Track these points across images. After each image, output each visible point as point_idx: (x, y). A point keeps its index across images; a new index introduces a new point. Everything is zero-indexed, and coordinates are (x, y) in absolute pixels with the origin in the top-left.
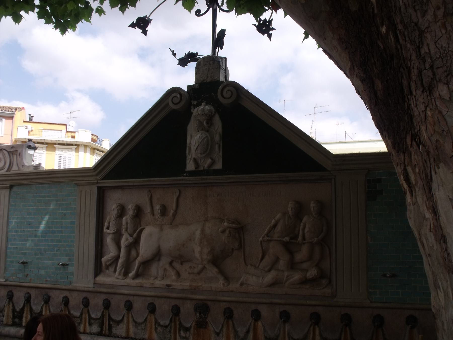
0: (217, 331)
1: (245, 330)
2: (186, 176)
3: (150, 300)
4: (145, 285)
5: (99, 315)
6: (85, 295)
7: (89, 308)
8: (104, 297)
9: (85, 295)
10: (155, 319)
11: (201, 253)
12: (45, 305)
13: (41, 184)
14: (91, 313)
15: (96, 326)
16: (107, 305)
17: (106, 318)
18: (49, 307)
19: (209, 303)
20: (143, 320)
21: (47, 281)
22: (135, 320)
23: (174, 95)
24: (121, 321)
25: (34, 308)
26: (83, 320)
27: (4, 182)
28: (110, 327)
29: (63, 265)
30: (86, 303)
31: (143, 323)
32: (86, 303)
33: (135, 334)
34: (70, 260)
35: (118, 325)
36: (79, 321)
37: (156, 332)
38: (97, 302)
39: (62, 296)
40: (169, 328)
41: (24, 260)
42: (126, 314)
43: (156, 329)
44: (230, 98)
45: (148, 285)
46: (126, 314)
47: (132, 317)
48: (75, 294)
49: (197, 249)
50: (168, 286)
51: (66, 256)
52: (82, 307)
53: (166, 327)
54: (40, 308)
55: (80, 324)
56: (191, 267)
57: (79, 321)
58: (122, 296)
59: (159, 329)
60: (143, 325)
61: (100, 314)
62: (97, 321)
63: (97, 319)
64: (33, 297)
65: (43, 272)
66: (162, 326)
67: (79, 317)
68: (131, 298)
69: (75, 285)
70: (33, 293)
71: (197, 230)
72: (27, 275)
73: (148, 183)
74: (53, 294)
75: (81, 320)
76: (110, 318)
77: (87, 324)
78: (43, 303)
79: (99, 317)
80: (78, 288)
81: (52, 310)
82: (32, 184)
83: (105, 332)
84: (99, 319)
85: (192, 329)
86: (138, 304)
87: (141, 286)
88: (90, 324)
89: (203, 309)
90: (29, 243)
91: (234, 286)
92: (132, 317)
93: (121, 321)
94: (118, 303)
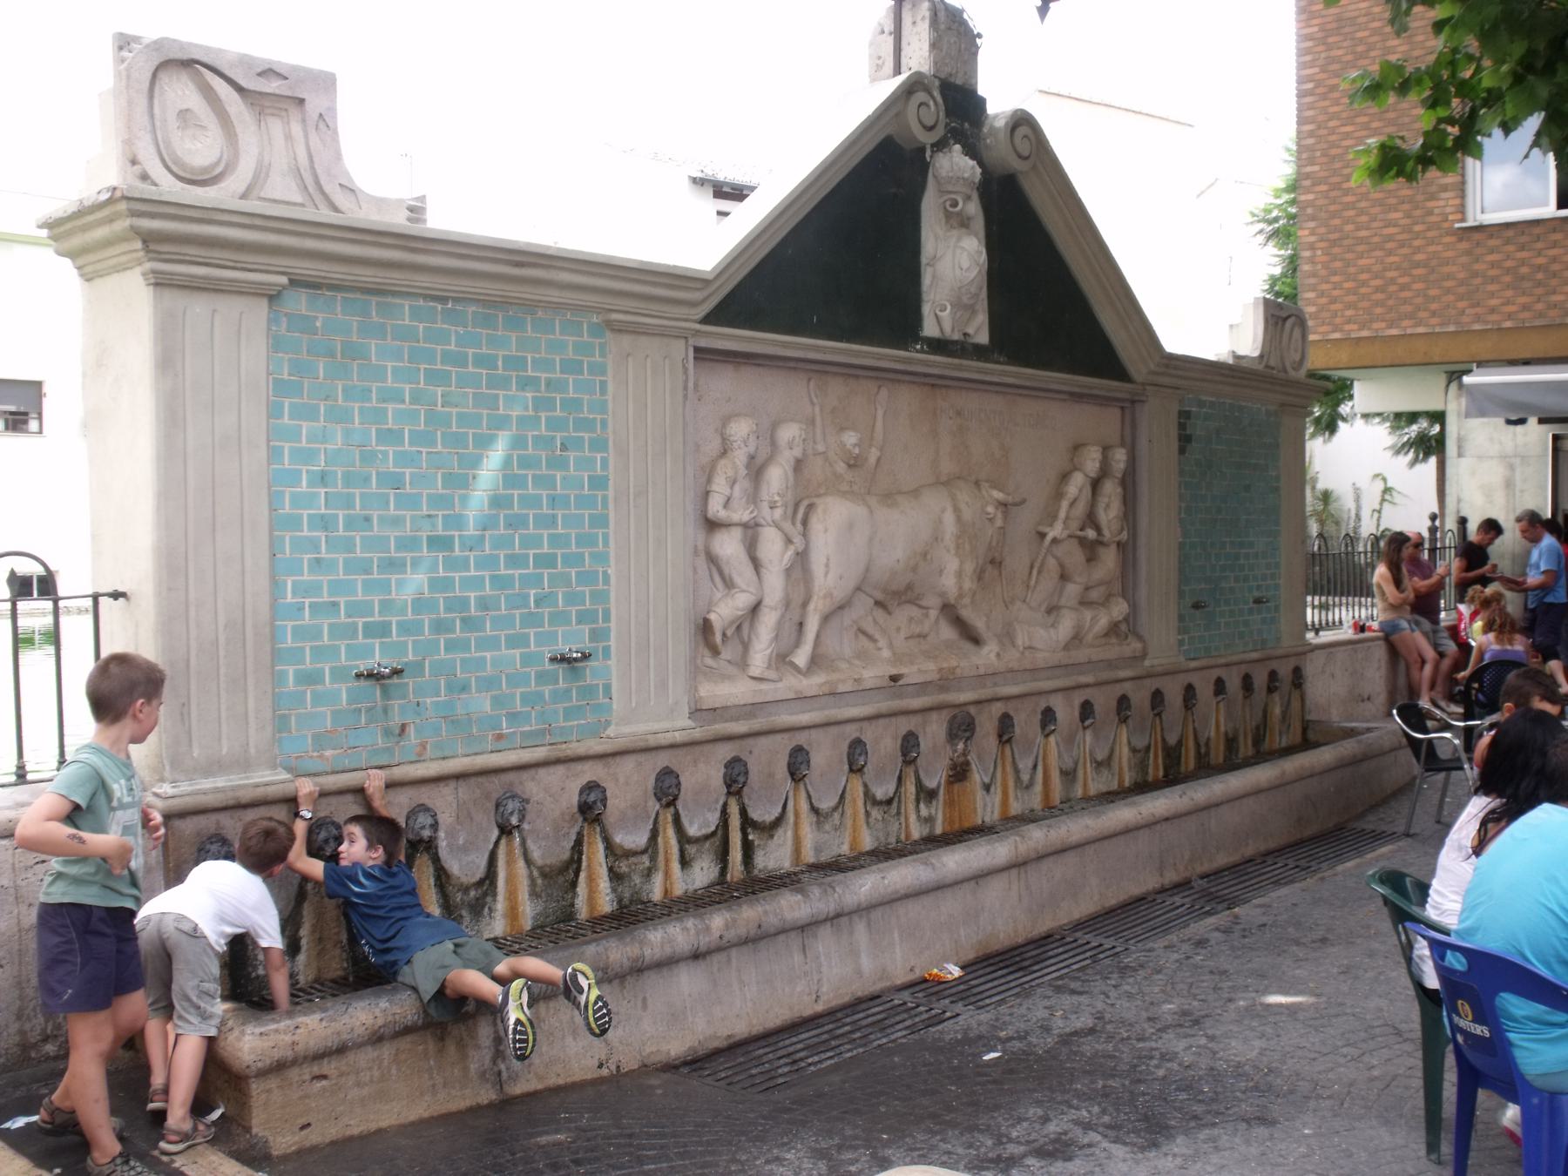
0: (987, 780)
1: (1030, 764)
2: (922, 351)
3: (852, 731)
4: (841, 688)
5: (713, 819)
6: (662, 760)
7: (680, 805)
8: (725, 752)
9: (662, 760)
10: (865, 786)
11: (959, 574)
12: (503, 841)
13: (443, 300)
14: (685, 821)
15: (705, 864)
16: (735, 780)
17: (735, 822)
18: (523, 843)
19: (972, 710)
20: (837, 799)
21: (500, 737)
22: (816, 804)
23: (921, 96)
24: (778, 822)
25: (454, 866)
26: (661, 858)
27: (192, 251)
28: (748, 848)
29: (563, 659)
30: (667, 790)
31: (835, 809)
32: (667, 790)
33: (818, 850)
34: (596, 635)
35: (772, 837)
36: (647, 864)
37: (868, 823)
38: (703, 775)
39: (575, 787)
40: (895, 804)
41: (377, 659)
42: (791, 794)
43: (868, 814)
44: (1020, 156)
45: (848, 687)
46: (791, 794)
47: (809, 797)
48: (628, 765)
49: (952, 564)
50: (894, 679)
51: (579, 622)
52: (654, 806)
53: (889, 802)
54: (483, 862)
55: (648, 873)
56: (911, 619)
57: (647, 864)
58: (778, 737)
59: (876, 813)
60: (836, 815)
61: (717, 814)
62: (707, 844)
63: (707, 837)
64: (445, 819)
65: (481, 703)
66: (880, 803)
67: (644, 852)
68: (801, 739)
69: (626, 730)
70: (444, 802)
71: (943, 511)
72: (403, 728)
73: (812, 355)
74: (533, 786)
75: (653, 859)
76: (747, 822)
77: (675, 866)
78: (496, 832)
79: (713, 828)
80: (652, 741)
81: (536, 854)
82: (394, 294)
83: (591, 899)
84: (714, 834)
85: (942, 792)
86: (826, 755)
87: (833, 694)
88: (685, 863)
89: (962, 726)
90: (415, 582)
91: (988, 656)
92: (809, 797)
93: (778, 822)
94: (768, 759)
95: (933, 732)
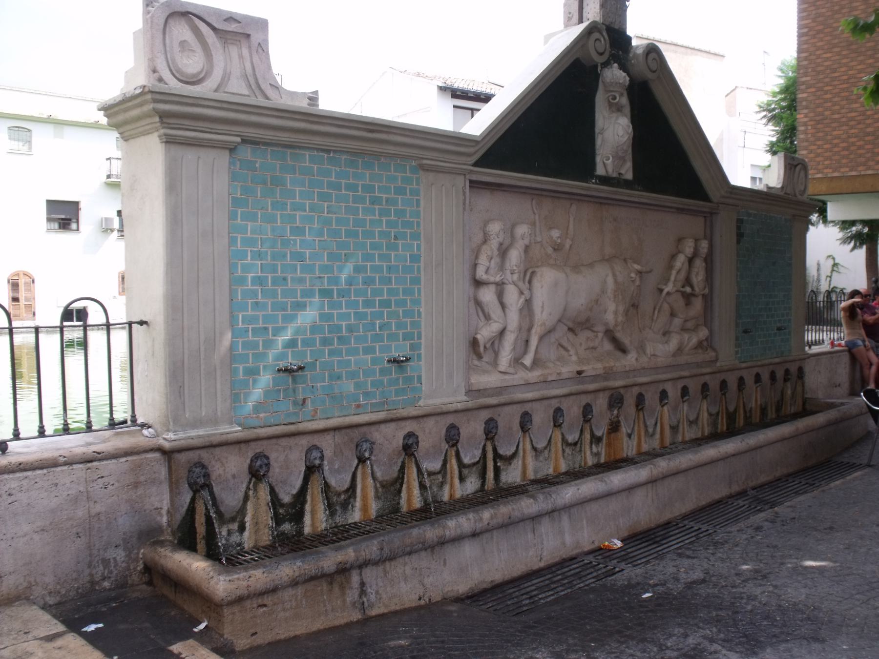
0: (629, 431)
1: (653, 422)
2: (596, 183)
3: (555, 403)
4: (550, 378)
5: (478, 453)
8: (485, 415)
10: (563, 435)
11: (616, 313)
12: (360, 467)
13: (328, 151)
14: (462, 455)
15: (473, 480)
16: (491, 431)
17: (490, 455)
19: (622, 391)
21: (358, 406)
22: (535, 445)
23: (596, 35)
24: (514, 455)
25: (333, 482)
26: (449, 476)
27: (187, 122)
28: (497, 471)
29: (394, 361)
30: (452, 437)
31: (545, 448)
32: (452, 437)
33: (536, 472)
35: (510, 464)
36: (441, 480)
37: (564, 456)
38: (472, 429)
39: (401, 435)
40: (579, 445)
42: (521, 440)
46: (521, 440)
47: (531, 441)
48: (430, 423)
49: (612, 307)
50: (579, 373)
51: (404, 339)
53: (575, 444)
55: (442, 485)
56: (588, 338)
57: (441, 480)
58: (515, 406)
59: (568, 450)
60: (546, 452)
61: (480, 451)
62: (474, 469)
63: (474, 464)
64: (328, 453)
65: (349, 387)
68: (527, 407)
69: (430, 402)
70: (327, 444)
71: (607, 276)
72: (304, 400)
75: (444, 477)
76: (497, 456)
77: (457, 481)
78: (356, 461)
79: (478, 459)
80: (445, 408)
81: (379, 474)
82: (300, 148)
84: (478, 462)
86: (541, 417)
87: (545, 382)
88: (462, 479)
89: (616, 401)
91: (631, 360)
92: (531, 441)
93: (514, 455)
94: (509, 419)
95: (600, 404)
